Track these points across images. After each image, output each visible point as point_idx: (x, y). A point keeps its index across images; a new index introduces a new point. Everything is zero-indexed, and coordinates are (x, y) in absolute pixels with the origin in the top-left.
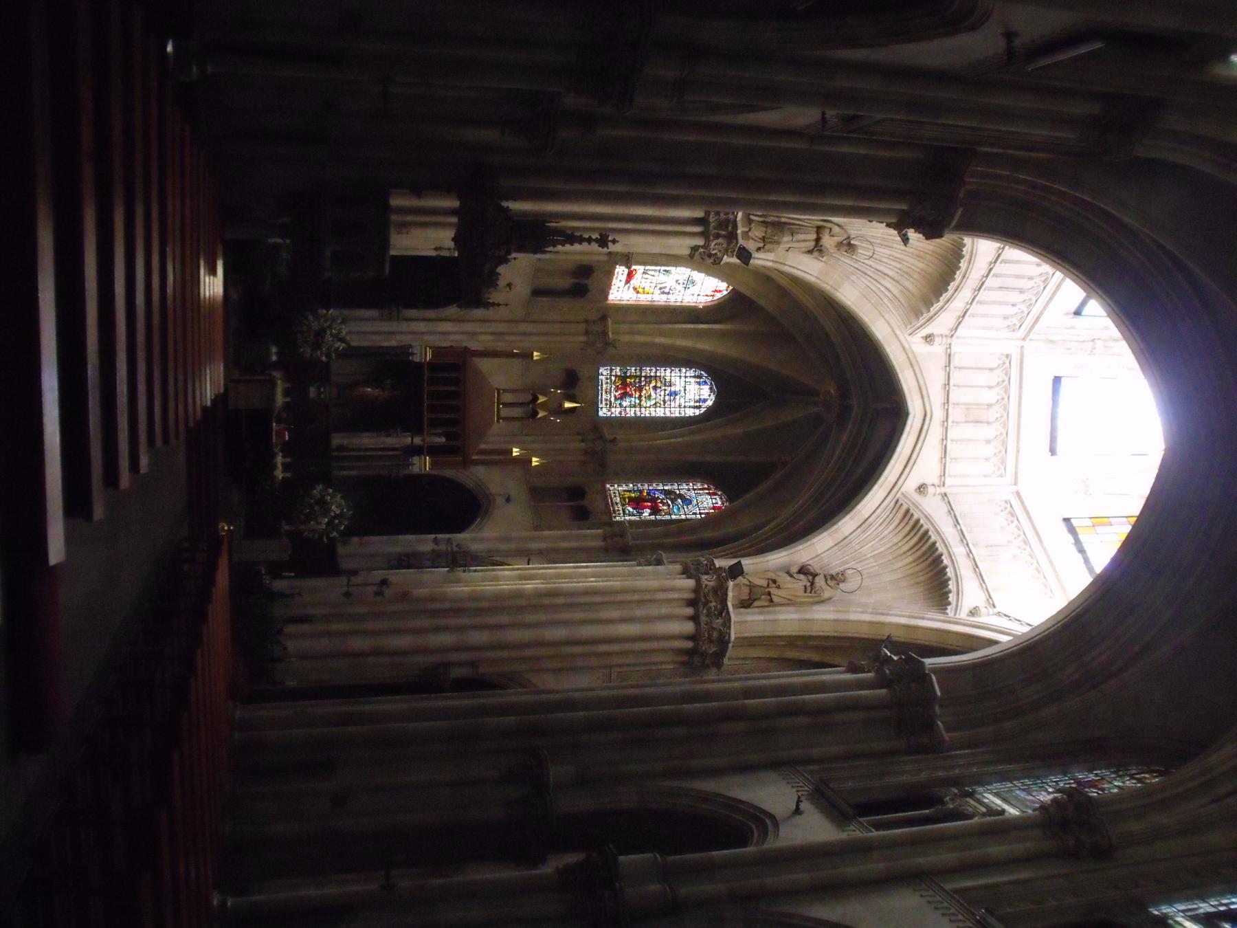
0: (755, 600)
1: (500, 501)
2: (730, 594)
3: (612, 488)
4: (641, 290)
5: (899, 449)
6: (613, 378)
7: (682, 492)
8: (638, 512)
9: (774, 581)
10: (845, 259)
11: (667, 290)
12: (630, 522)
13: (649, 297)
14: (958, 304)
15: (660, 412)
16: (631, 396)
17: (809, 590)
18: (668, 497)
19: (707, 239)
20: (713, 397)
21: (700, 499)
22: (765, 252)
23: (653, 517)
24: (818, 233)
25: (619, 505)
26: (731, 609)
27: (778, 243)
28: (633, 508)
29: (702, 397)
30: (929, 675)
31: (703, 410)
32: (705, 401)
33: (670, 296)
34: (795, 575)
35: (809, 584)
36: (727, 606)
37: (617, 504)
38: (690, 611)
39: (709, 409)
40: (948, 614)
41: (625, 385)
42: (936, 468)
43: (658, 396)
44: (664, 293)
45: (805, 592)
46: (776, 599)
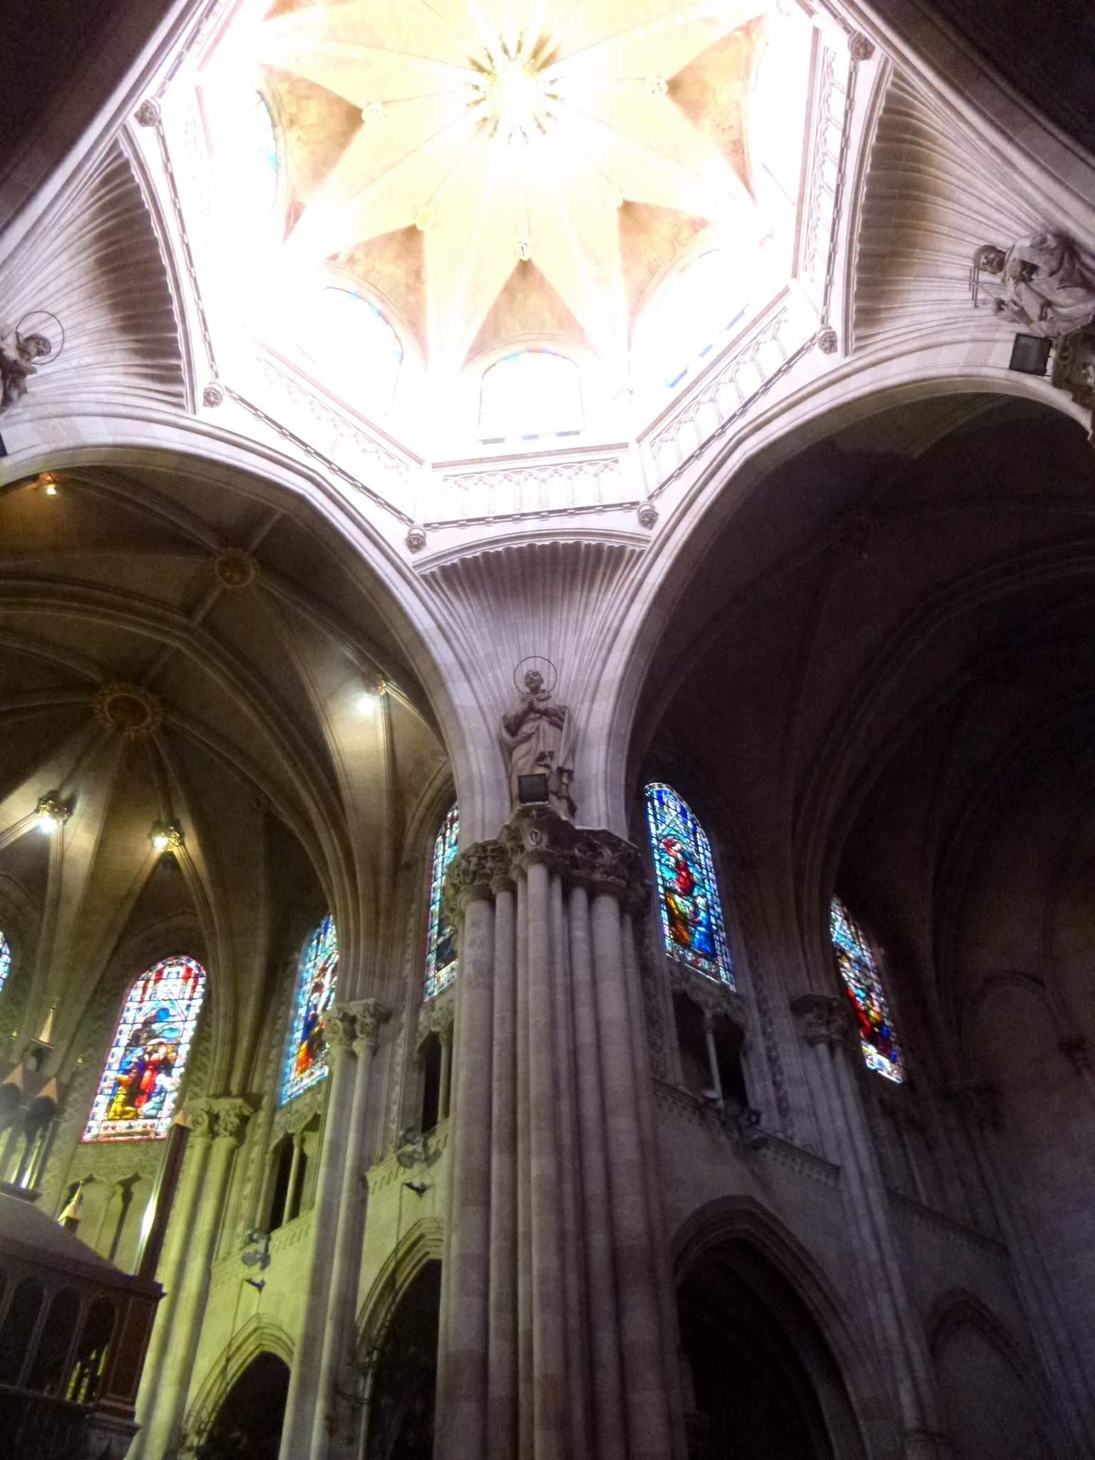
3: (94, 1132)
7: (141, 1019)
8: (159, 1094)
18: (142, 1042)
21: (160, 995)
28: (149, 1099)
37: (130, 1127)
38: (580, 896)
45: (561, 728)
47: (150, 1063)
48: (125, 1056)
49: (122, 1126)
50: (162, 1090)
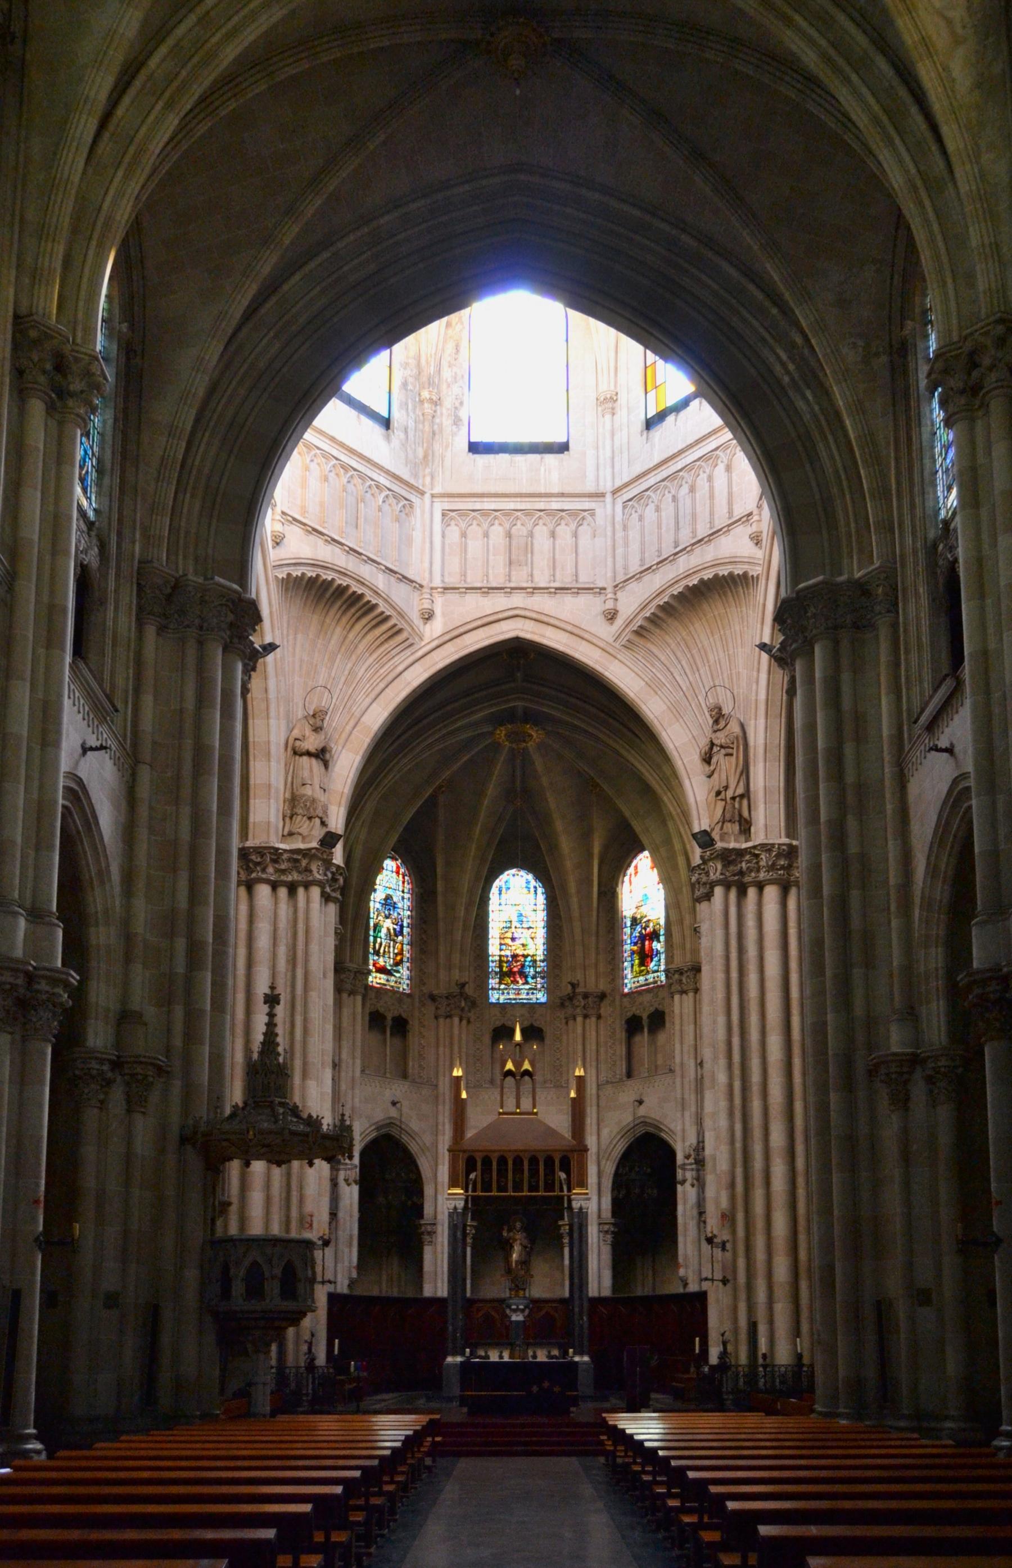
0: (740, 815)
1: (642, 1111)
2: (732, 845)
3: (629, 986)
4: (399, 958)
5: (561, 648)
6: (503, 986)
9: (718, 793)
10: (333, 722)
11: (398, 928)
12: (667, 964)
13: (406, 948)
14: (380, 581)
15: (541, 933)
16: (523, 966)
17: (730, 751)
19: (307, 886)
20: (522, 873)
22: (327, 816)
23: (662, 938)
24: (301, 755)
25: (648, 977)
26: (750, 844)
27: (314, 801)
28: (652, 961)
29: (525, 885)
30: (798, 593)
31: (538, 884)
32: (528, 882)
33: (405, 924)
34: (712, 768)
35: (723, 751)
36: (746, 849)
39: (537, 878)
40: (758, 576)
41: (511, 973)
42: (583, 599)
43: (524, 936)
44: (401, 933)
46: (740, 790)
47: (646, 935)
48: (631, 933)
49: (642, 979)
50: (658, 952)
